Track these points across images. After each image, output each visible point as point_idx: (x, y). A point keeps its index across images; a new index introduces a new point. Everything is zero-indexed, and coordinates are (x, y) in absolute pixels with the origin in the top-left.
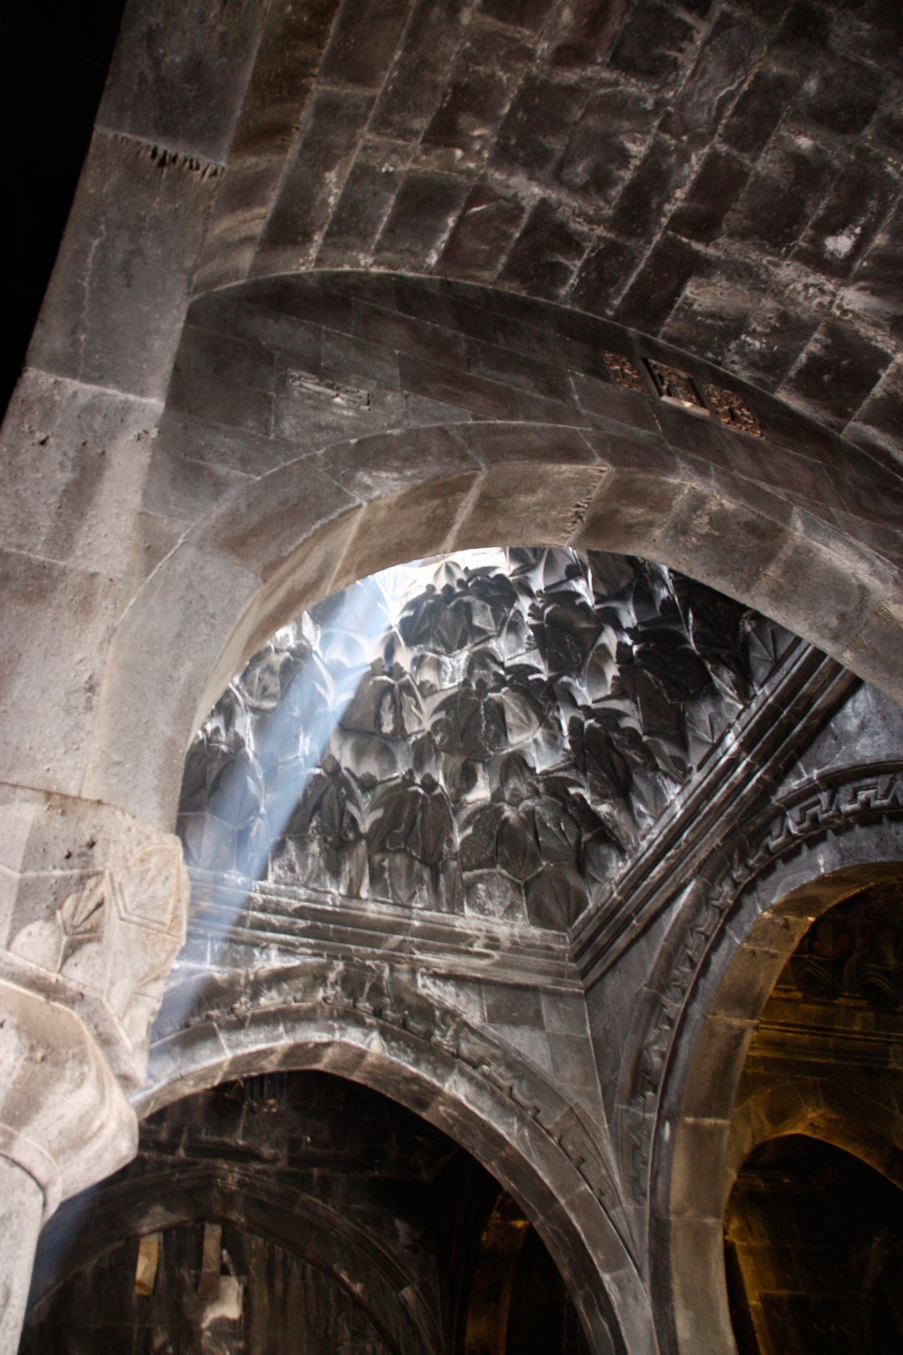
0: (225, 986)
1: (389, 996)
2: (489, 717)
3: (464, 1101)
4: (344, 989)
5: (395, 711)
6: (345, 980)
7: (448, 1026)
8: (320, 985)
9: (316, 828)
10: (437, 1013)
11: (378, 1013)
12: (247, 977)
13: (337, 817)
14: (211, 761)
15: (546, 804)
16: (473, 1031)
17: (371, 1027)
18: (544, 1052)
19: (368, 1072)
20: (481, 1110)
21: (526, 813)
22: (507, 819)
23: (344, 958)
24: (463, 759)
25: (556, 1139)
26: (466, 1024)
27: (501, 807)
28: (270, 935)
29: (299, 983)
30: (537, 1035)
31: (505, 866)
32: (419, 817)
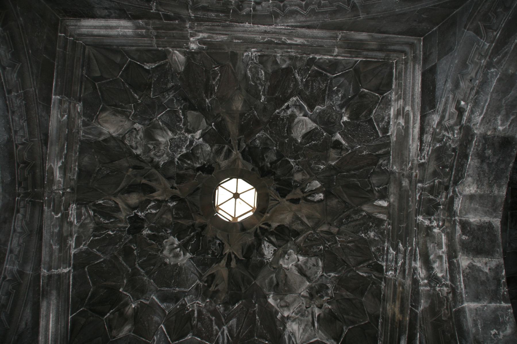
0: (430, 301)
1: (434, 181)
2: (310, 140)
3: (482, 116)
4: (433, 215)
5: (314, 193)
6: (429, 213)
7: (444, 136)
8: (431, 231)
9: (365, 234)
10: (438, 145)
11: (447, 188)
12: (425, 285)
13: (358, 222)
14: (342, 296)
15: (331, 100)
16: (443, 117)
17: (454, 191)
18: (445, 62)
19: (490, 186)
20: (486, 101)
21: (341, 109)
22: (349, 118)
23: (416, 217)
24: (331, 150)
25: (495, 33)
26: (439, 123)
27: (343, 122)
28: (407, 267)
29: (431, 246)
30: (439, 70)
31: (371, 112)
32: (353, 172)
